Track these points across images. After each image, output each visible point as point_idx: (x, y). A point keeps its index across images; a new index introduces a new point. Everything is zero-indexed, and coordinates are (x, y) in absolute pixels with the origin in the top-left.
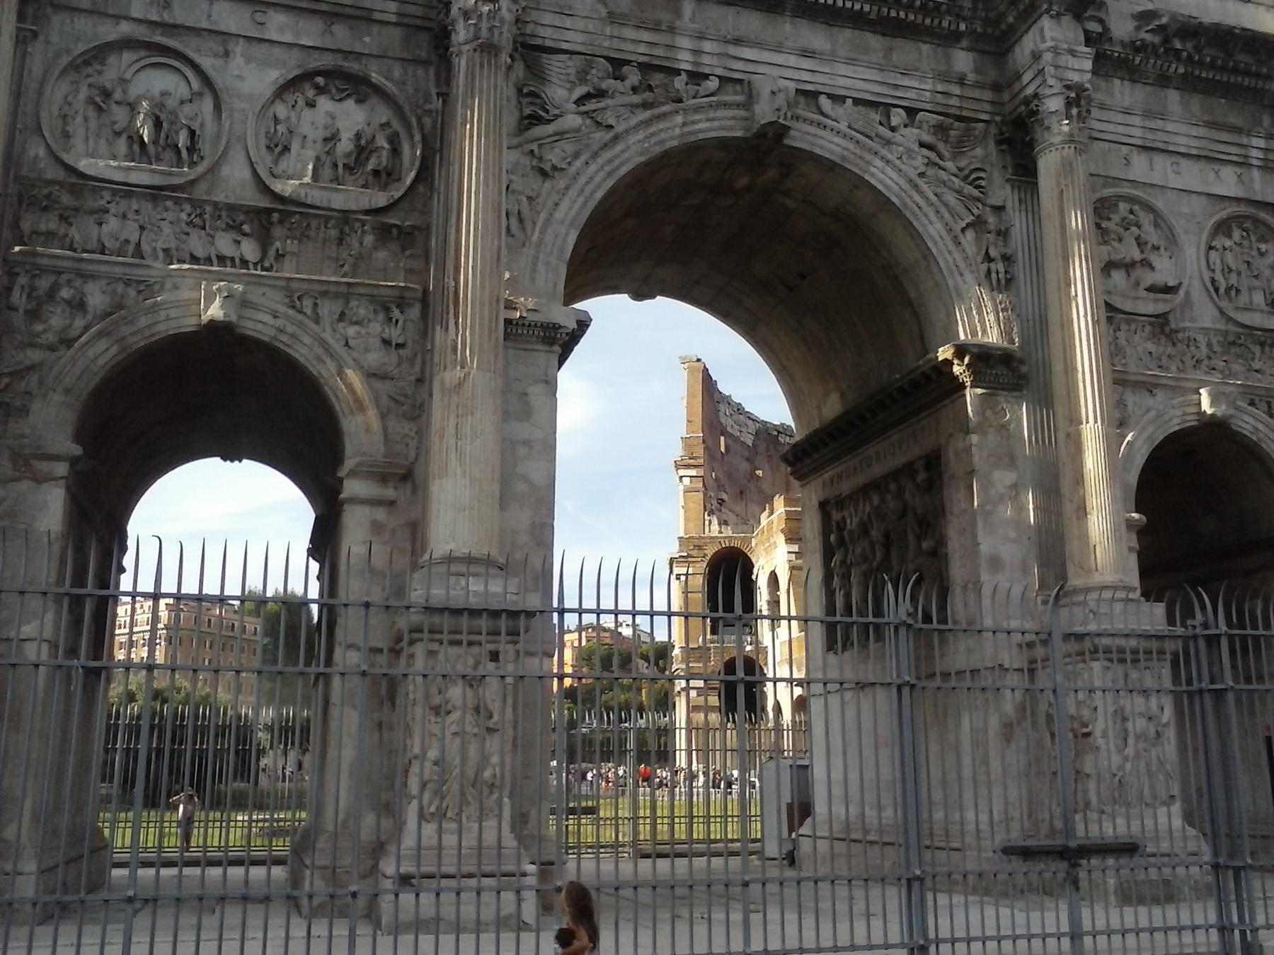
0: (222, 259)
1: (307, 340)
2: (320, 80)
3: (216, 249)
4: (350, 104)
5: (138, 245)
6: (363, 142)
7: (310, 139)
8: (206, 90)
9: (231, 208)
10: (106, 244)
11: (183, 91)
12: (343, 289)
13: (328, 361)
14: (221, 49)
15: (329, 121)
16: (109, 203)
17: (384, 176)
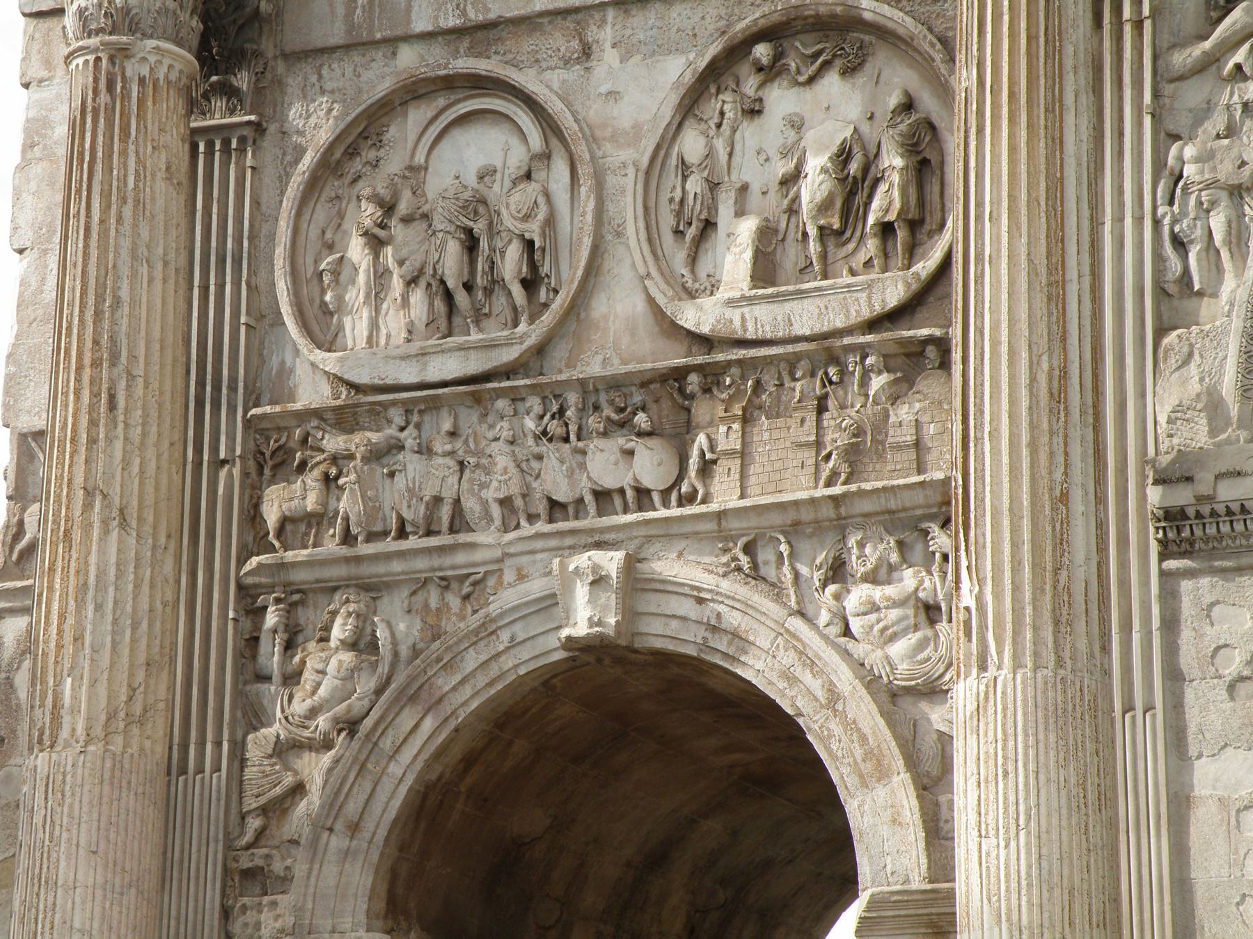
0: (603, 496)
1: (763, 639)
2: (762, 51)
3: (589, 478)
4: (832, 82)
5: (457, 501)
6: (854, 167)
7: (755, 188)
8: (554, 142)
9: (615, 384)
10: (405, 515)
11: (517, 157)
12: (828, 512)
13: (807, 678)
14: (575, 44)
15: (792, 135)
16: (402, 429)
17: (901, 234)
